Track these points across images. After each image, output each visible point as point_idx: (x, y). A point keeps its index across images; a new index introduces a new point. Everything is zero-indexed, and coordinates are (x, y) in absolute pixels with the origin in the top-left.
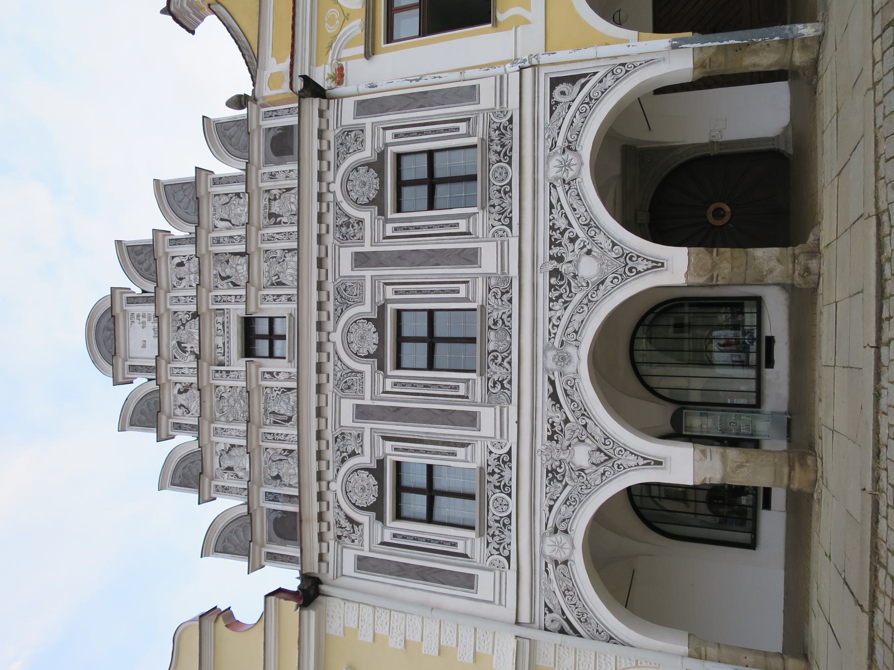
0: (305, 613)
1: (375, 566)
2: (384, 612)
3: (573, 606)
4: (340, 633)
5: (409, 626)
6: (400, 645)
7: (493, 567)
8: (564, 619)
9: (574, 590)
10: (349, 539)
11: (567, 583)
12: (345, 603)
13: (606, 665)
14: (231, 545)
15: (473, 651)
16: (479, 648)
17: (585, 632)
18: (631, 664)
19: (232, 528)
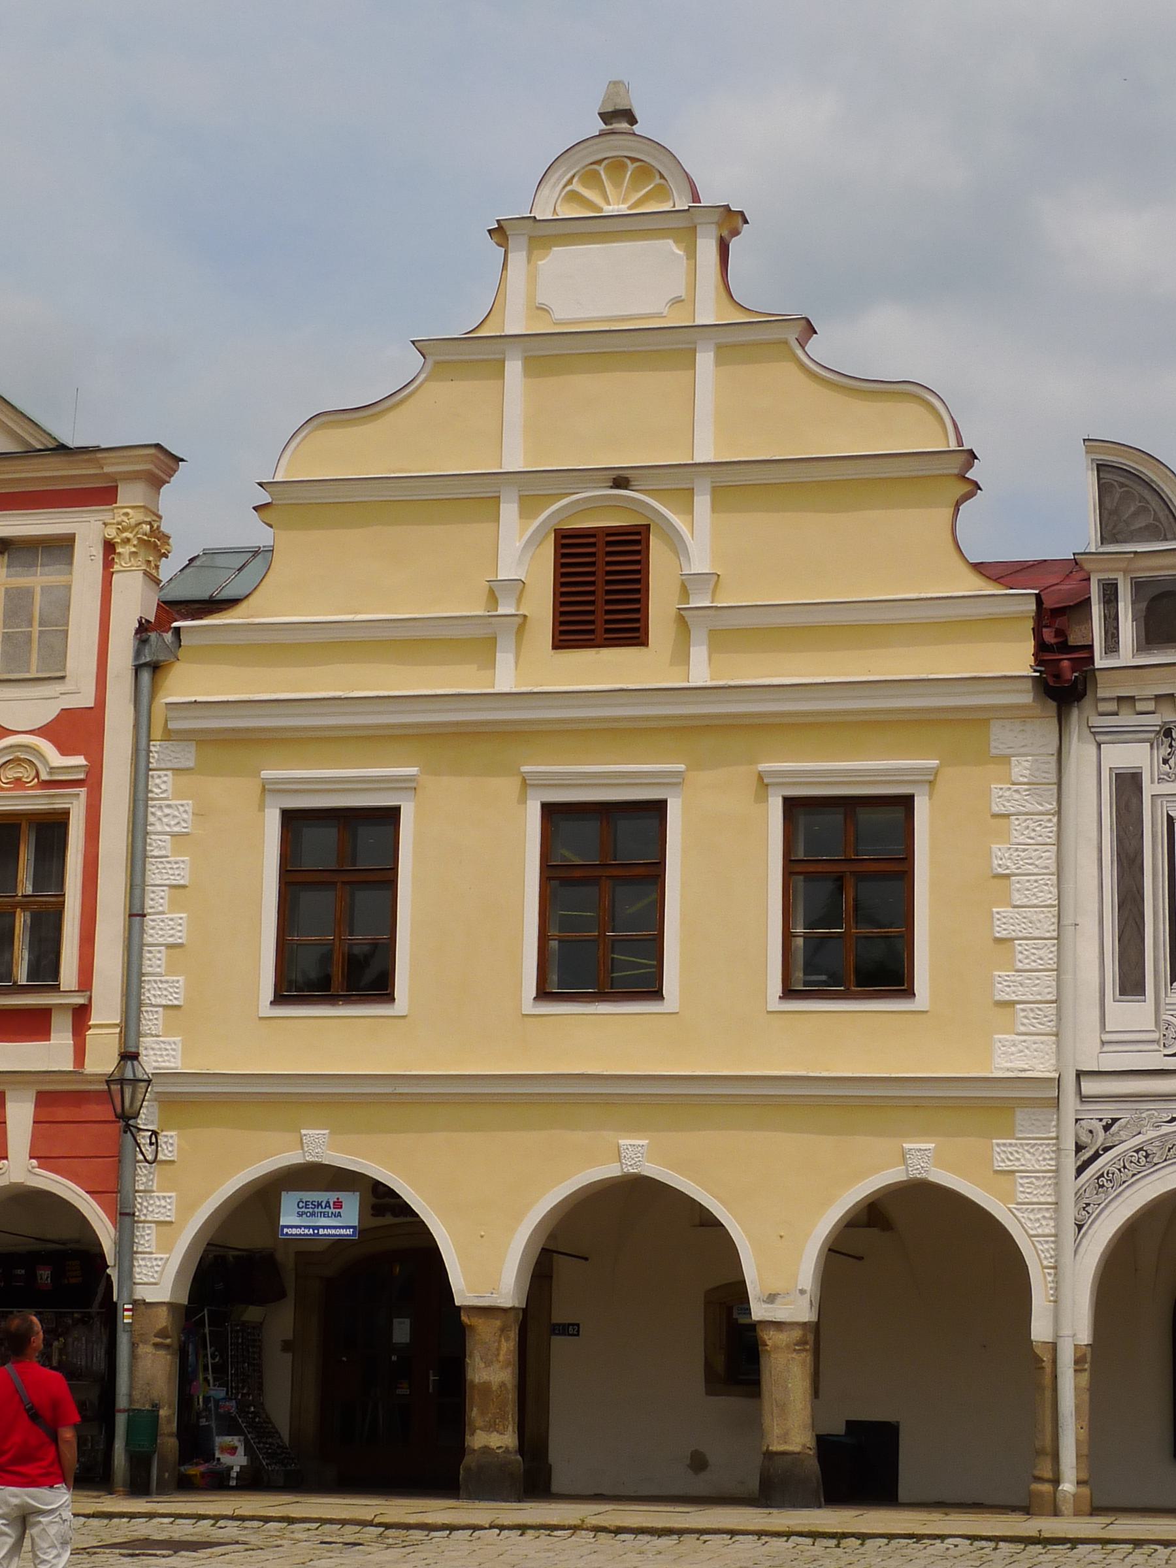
0: (1029, 685)
1: (1127, 806)
2: (1051, 832)
3: (1122, 1165)
4: (996, 748)
5: (1036, 881)
6: (1000, 865)
7: (1163, 1027)
8: (1097, 1151)
9: (1148, 1165)
10: (1169, 754)
11: (1159, 1154)
12: (1053, 755)
13: (1038, 1220)
14: (1116, 500)
15: (1016, 998)
16: (1023, 1010)
17: (1083, 1185)
18: (1046, 1258)
19: (1151, 502)
